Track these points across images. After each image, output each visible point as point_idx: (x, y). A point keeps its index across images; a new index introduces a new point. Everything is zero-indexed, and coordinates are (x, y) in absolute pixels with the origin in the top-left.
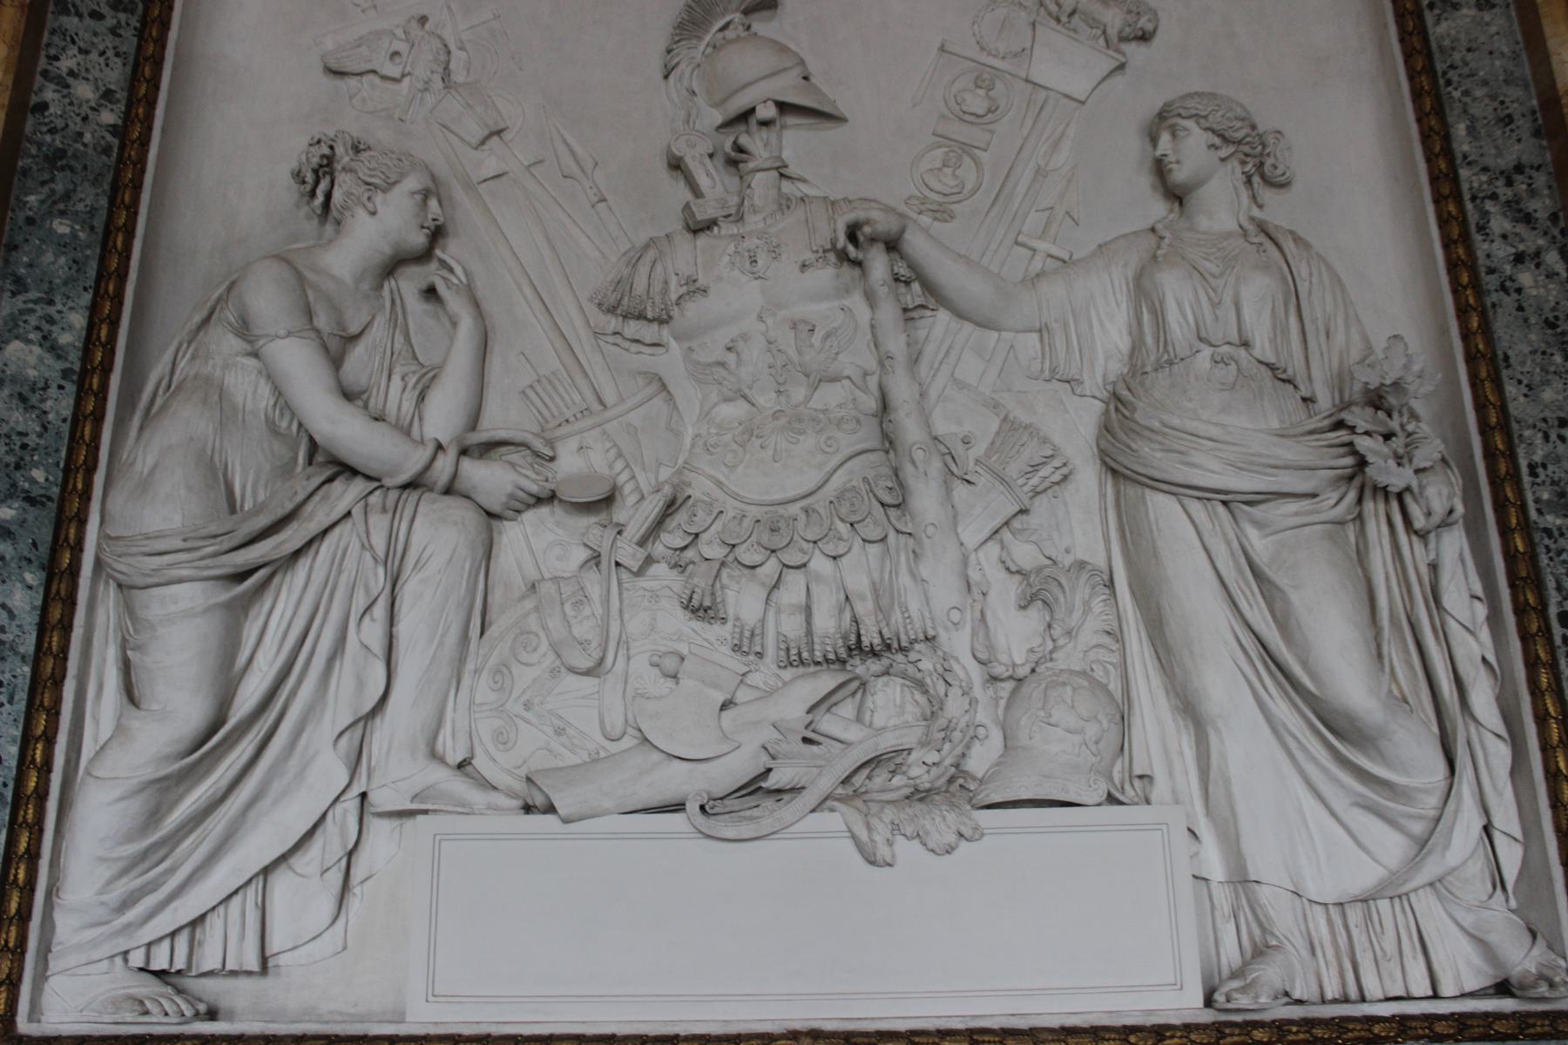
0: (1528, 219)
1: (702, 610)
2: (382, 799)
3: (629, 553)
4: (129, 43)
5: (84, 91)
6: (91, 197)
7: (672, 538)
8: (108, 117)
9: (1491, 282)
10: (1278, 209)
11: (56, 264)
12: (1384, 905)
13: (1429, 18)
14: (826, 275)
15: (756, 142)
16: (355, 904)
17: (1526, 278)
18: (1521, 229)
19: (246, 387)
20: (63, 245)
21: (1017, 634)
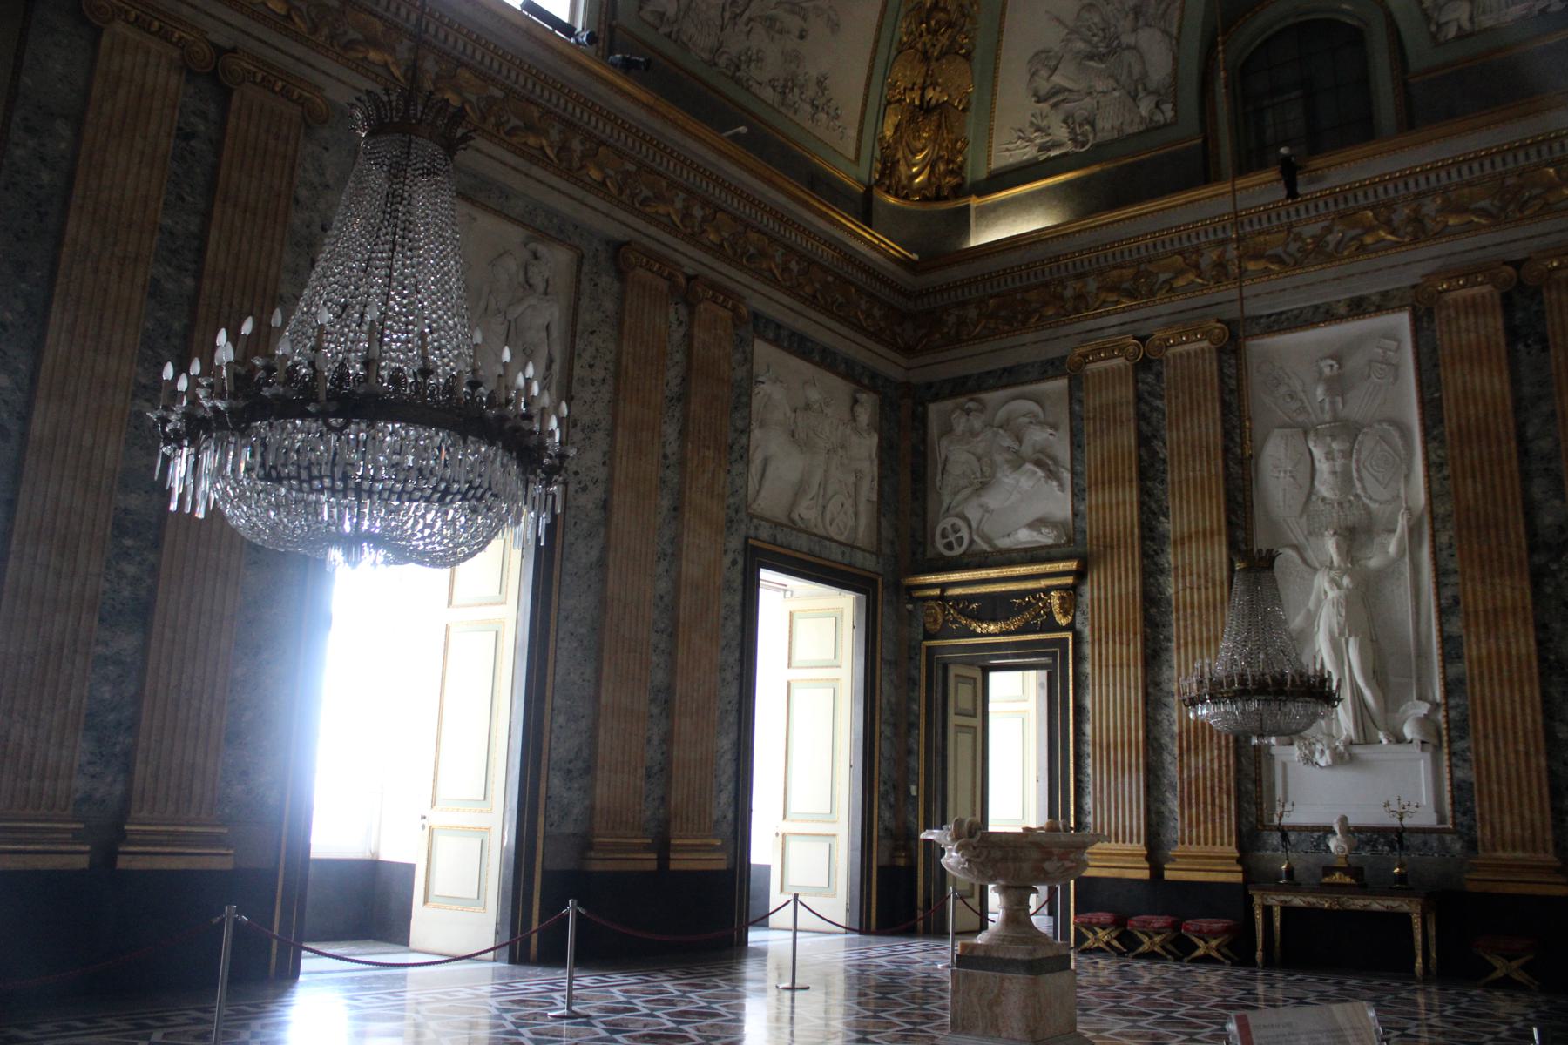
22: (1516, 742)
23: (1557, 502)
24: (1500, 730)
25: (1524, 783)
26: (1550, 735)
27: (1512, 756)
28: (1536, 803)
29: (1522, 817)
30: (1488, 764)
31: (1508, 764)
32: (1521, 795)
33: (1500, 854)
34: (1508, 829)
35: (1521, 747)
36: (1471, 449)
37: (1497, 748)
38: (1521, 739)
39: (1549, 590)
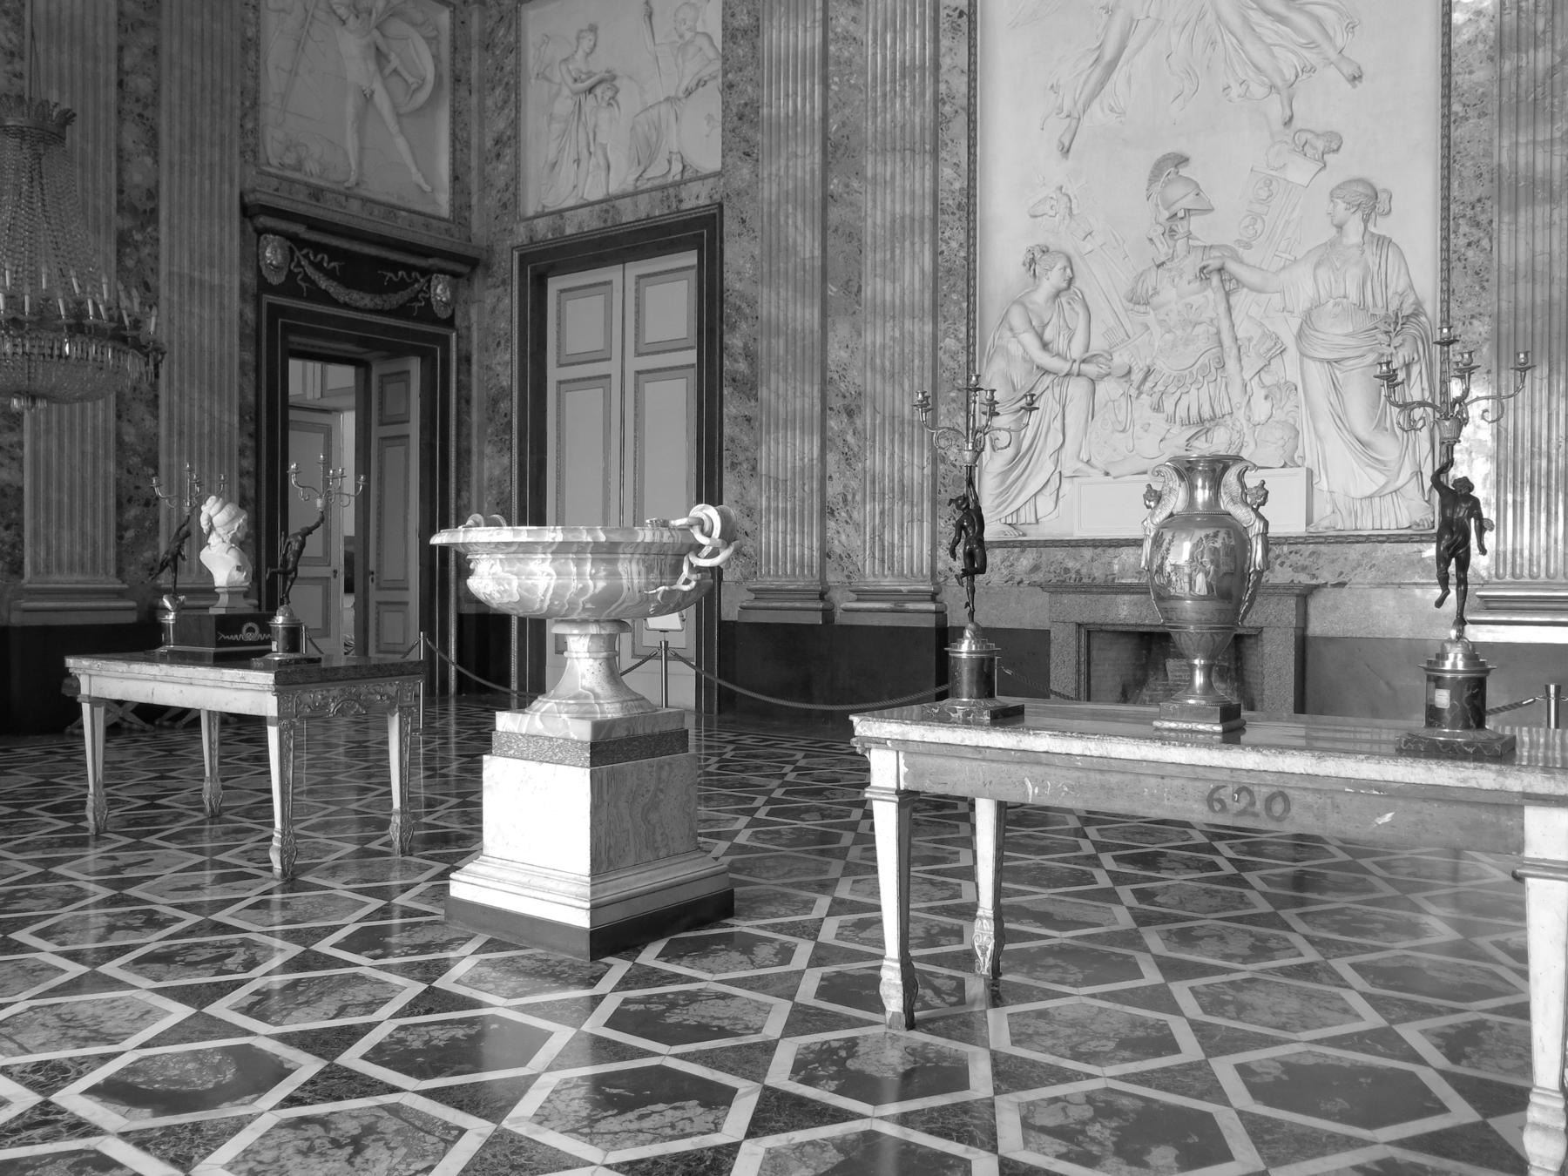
0: (1478, 224)
1: (1158, 408)
2: (1066, 473)
3: (1133, 392)
4: (965, 224)
5: (954, 244)
6: (962, 285)
7: (1149, 384)
8: (963, 254)
9: (1454, 257)
10: (1381, 227)
11: (954, 310)
12: (1377, 499)
13: (1453, 127)
14: (1196, 285)
15: (1181, 228)
16: (1061, 503)
17: (1470, 253)
18: (1474, 230)
19: (1014, 348)
20: (957, 303)
21: (1261, 409)
22: (83, 440)
23: (148, 160)
24: (66, 425)
25: (89, 492)
26: (120, 441)
27: (78, 456)
28: (100, 516)
29: (83, 534)
30: (48, 465)
31: (72, 468)
32: (83, 506)
33: (56, 577)
34: (66, 546)
35: (89, 448)
36: (60, 51)
37: (61, 447)
38: (89, 438)
39: (130, 263)
